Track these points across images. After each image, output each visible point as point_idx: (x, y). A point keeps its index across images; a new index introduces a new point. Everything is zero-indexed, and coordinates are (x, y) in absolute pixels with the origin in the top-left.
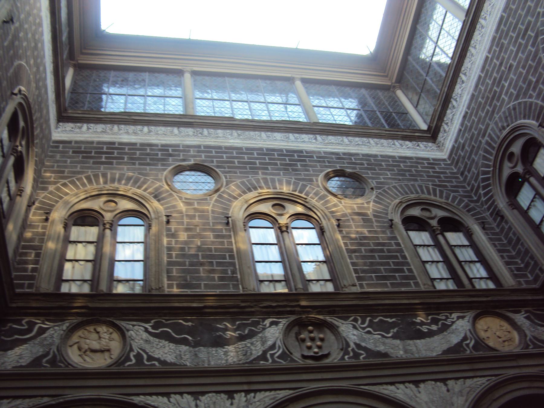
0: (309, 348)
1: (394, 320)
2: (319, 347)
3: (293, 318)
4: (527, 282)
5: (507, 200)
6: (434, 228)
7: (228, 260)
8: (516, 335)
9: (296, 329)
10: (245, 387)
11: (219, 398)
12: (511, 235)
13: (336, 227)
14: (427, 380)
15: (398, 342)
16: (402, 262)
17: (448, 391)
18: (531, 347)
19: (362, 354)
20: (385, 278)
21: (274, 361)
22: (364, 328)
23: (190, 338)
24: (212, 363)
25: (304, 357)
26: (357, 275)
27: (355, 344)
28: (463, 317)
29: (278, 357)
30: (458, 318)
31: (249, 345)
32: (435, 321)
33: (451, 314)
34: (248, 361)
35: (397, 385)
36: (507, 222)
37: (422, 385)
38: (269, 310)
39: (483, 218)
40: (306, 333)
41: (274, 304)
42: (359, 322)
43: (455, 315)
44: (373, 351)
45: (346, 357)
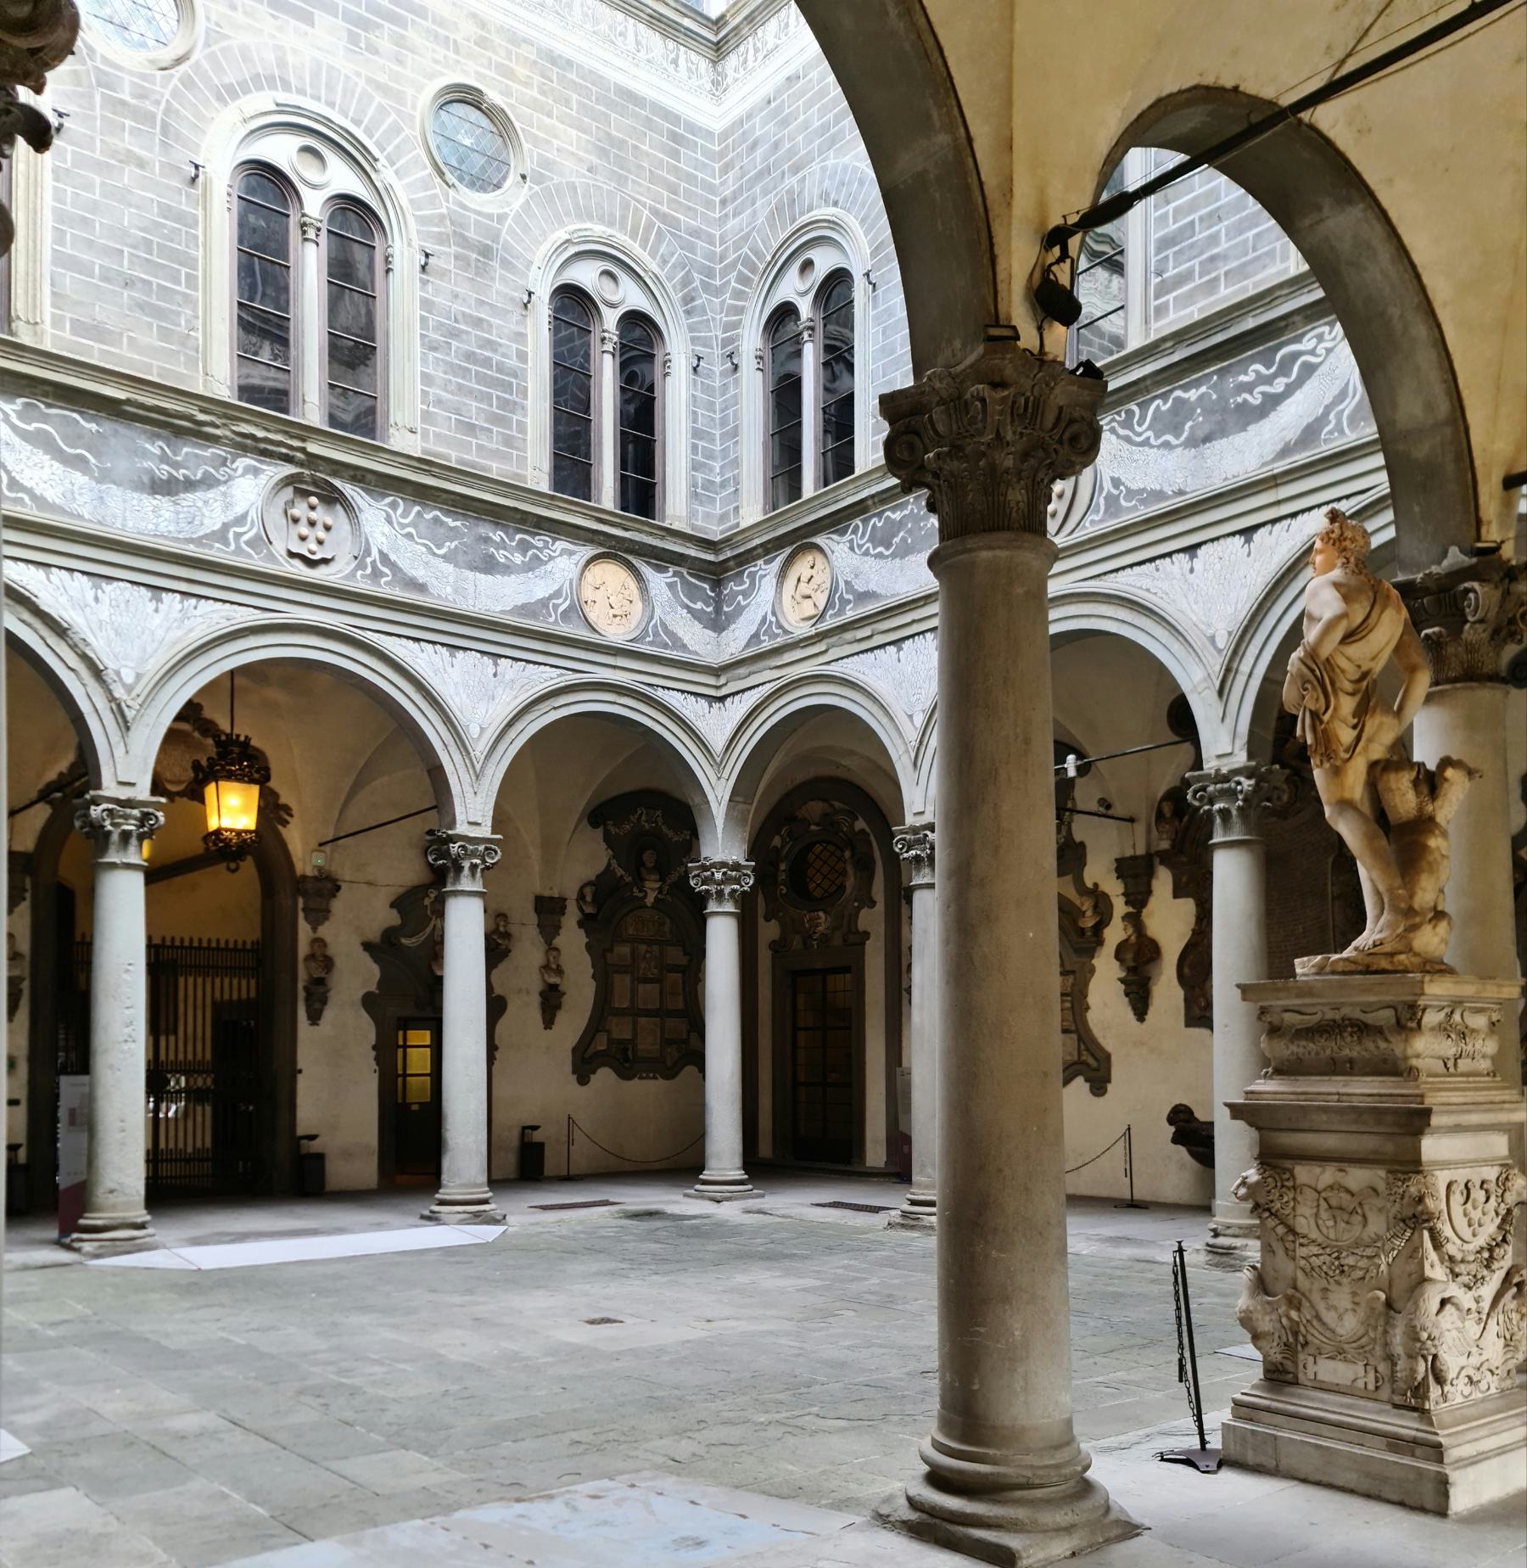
0: (303, 539)
1: (458, 523)
2: (320, 542)
3: (290, 469)
4: (707, 516)
5: (759, 345)
6: (606, 335)
7: (182, 288)
8: (638, 606)
9: (288, 493)
10: (184, 587)
11: (136, 593)
12: (731, 411)
13: (418, 268)
14: (471, 650)
15: (451, 567)
16: (515, 403)
17: (495, 675)
18: (651, 639)
19: (387, 575)
20: (470, 429)
21: (239, 551)
22: (403, 526)
23: (93, 460)
24: (130, 524)
25: (292, 555)
26: (425, 407)
27: (381, 552)
28: (571, 553)
29: (247, 543)
30: (564, 552)
31: (200, 504)
32: (524, 547)
33: (555, 540)
34: (194, 536)
35: (422, 643)
36: (736, 381)
37: (460, 654)
38: (249, 442)
39: (706, 343)
40: (305, 506)
41: (260, 434)
42: (400, 511)
43: (561, 545)
44: (405, 574)
45: (359, 573)
